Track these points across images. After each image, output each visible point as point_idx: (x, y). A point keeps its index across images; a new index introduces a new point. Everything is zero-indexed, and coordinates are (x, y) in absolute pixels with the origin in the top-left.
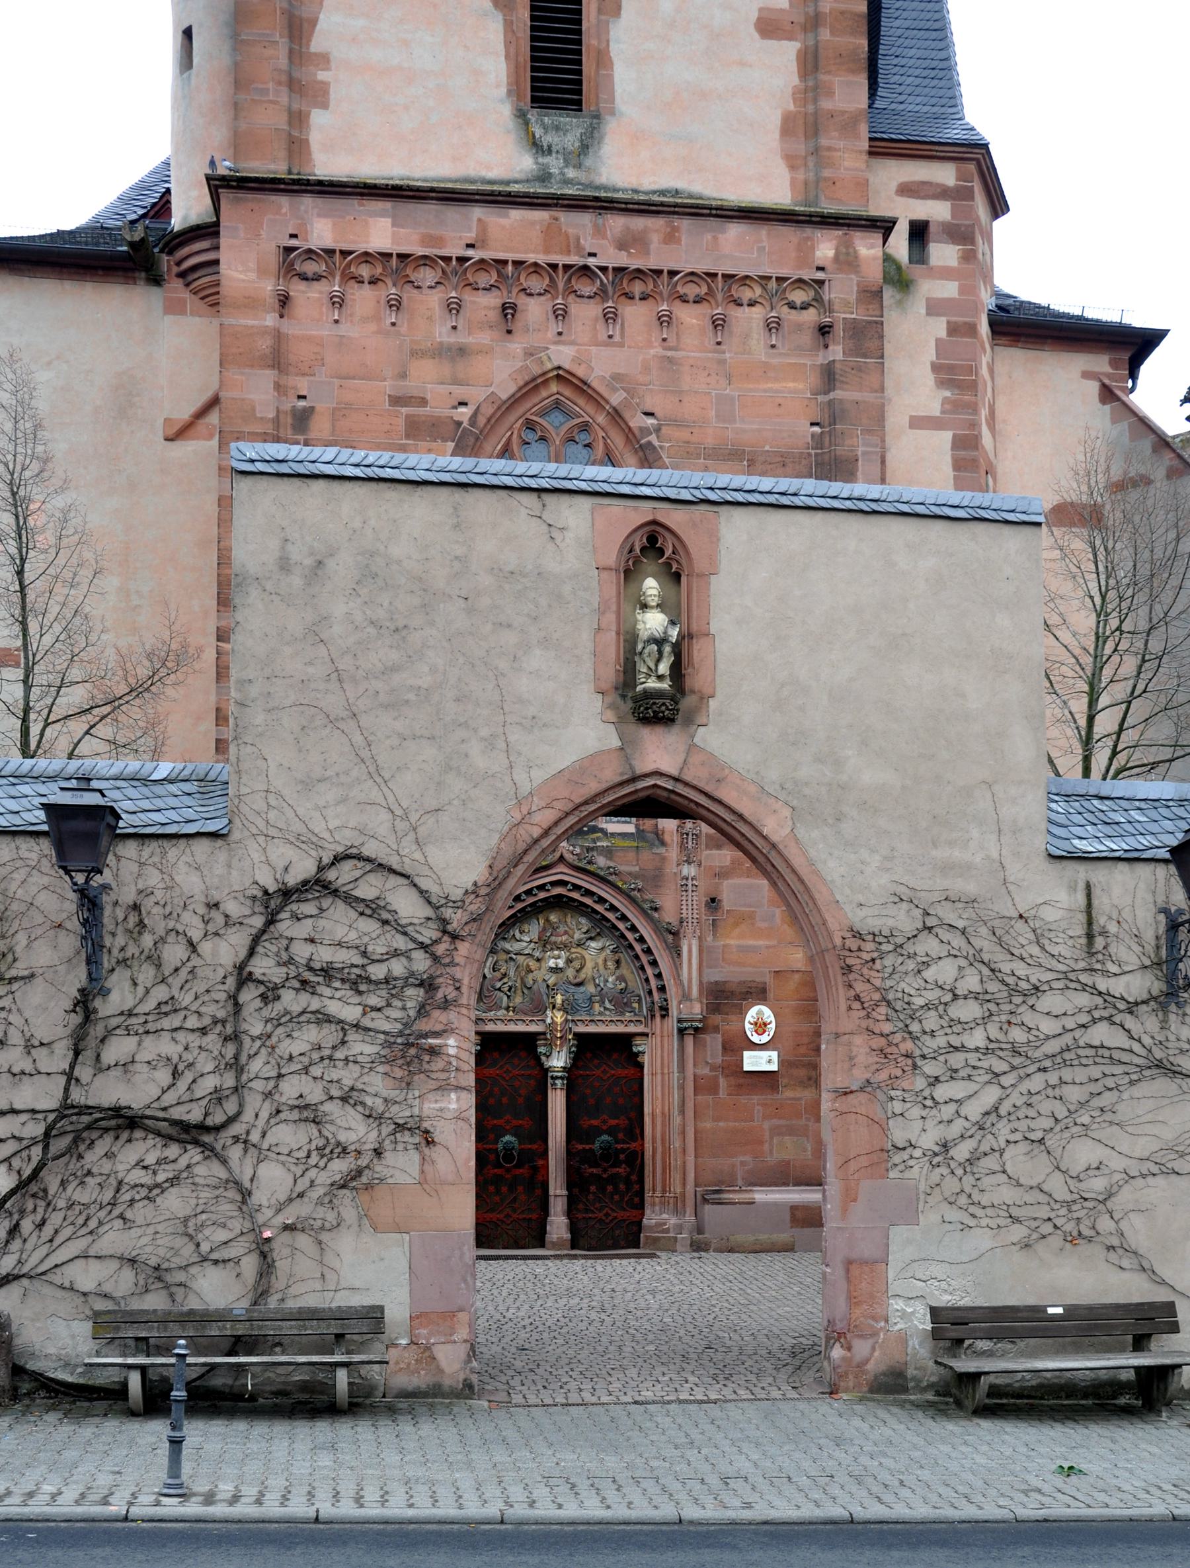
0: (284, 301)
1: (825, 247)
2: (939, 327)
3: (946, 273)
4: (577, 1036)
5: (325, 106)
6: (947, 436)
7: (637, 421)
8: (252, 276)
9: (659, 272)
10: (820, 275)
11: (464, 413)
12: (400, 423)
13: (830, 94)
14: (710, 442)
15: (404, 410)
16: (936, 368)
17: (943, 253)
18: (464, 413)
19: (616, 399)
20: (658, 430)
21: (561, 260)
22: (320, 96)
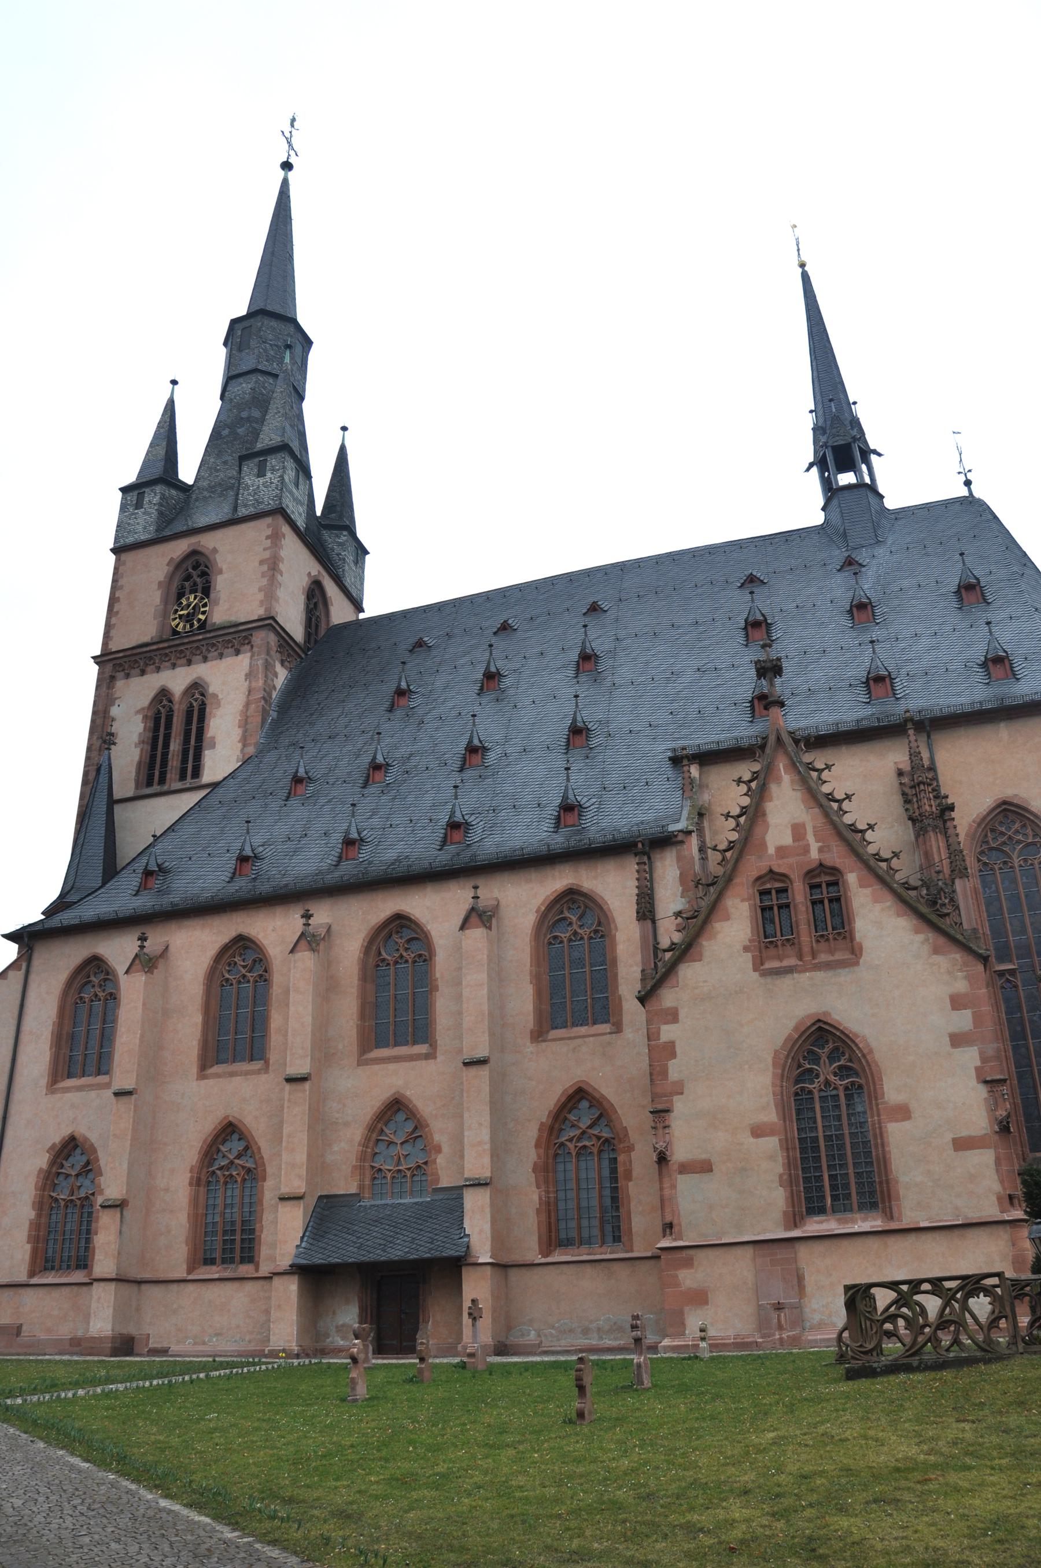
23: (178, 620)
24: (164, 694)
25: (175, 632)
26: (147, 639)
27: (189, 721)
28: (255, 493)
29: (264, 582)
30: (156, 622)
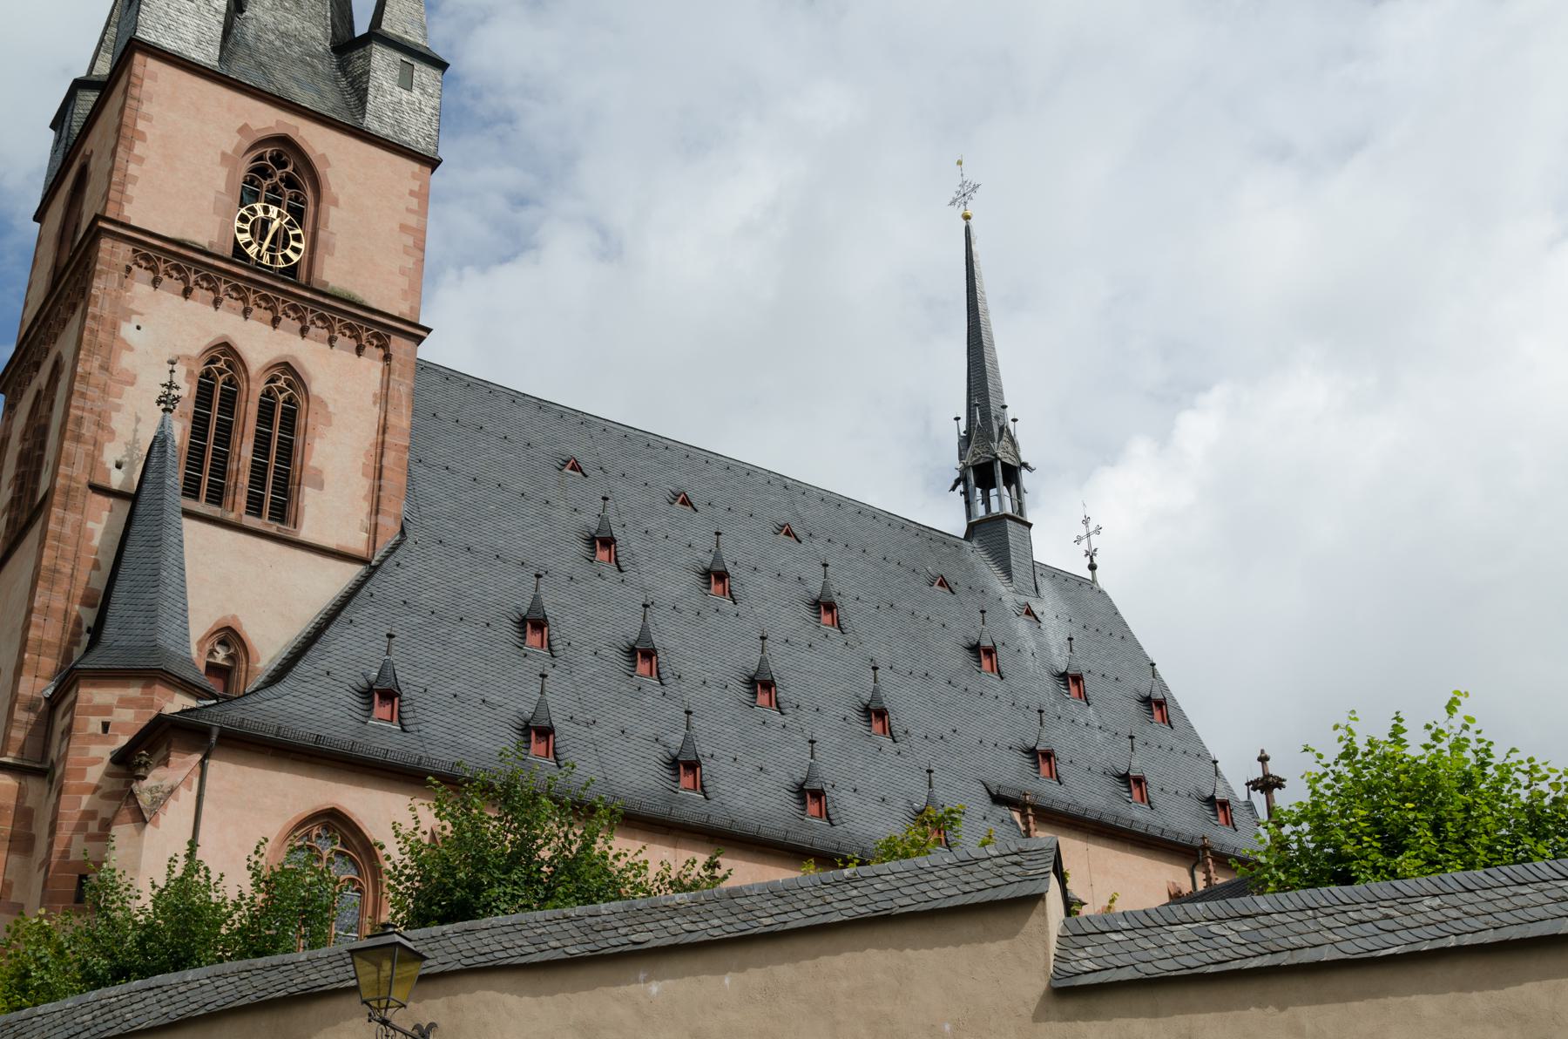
24: (225, 354)
25: (239, 251)
26: (202, 240)
28: (394, 110)
29: (409, 263)
30: (218, 219)
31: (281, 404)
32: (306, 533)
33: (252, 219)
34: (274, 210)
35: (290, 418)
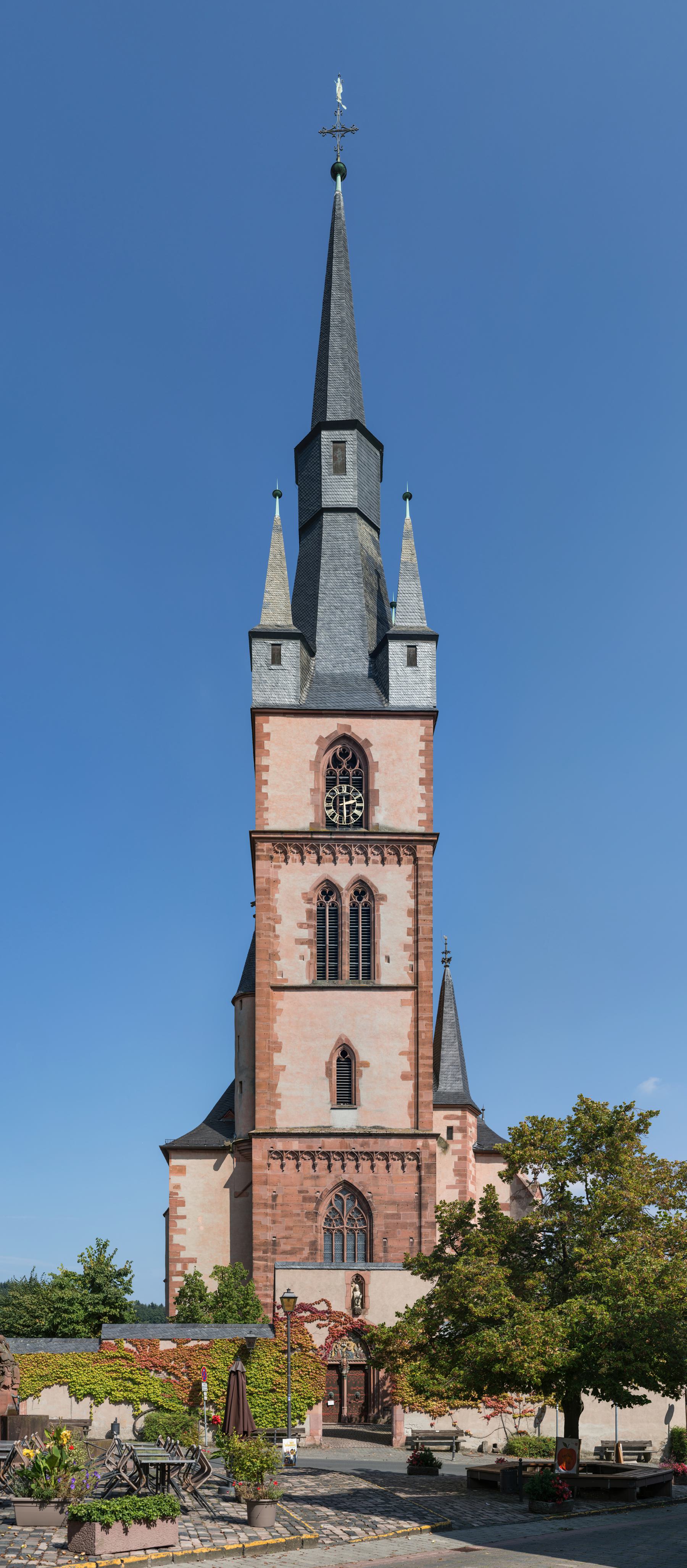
0: (269, 1165)
1: (420, 1143)
2: (456, 1158)
3: (458, 1142)
4: (350, 1365)
5: (280, 1108)
6: (457, 1191)
7: (366, 1195)
8: (261, 1159)
9: (372, 1152)
10: (418, 1151)
11: (318, 1195)
12: (301, 1198)
13: (422, 1096)
14: (386, 1200)
15: (302, 1194)
16: (454, 1171)
17: (457, 1136)
18: (318, 1195)
19: (360, 1189)
20: (372, 1197)
21: (345, 1150)
22: (278, 1105)
23: (332, 810)
27: (354, 922)
31: (361, 908)
32: (384, 981)
33: (333, 798)
34: (344, 787)
35: (369, 912)
